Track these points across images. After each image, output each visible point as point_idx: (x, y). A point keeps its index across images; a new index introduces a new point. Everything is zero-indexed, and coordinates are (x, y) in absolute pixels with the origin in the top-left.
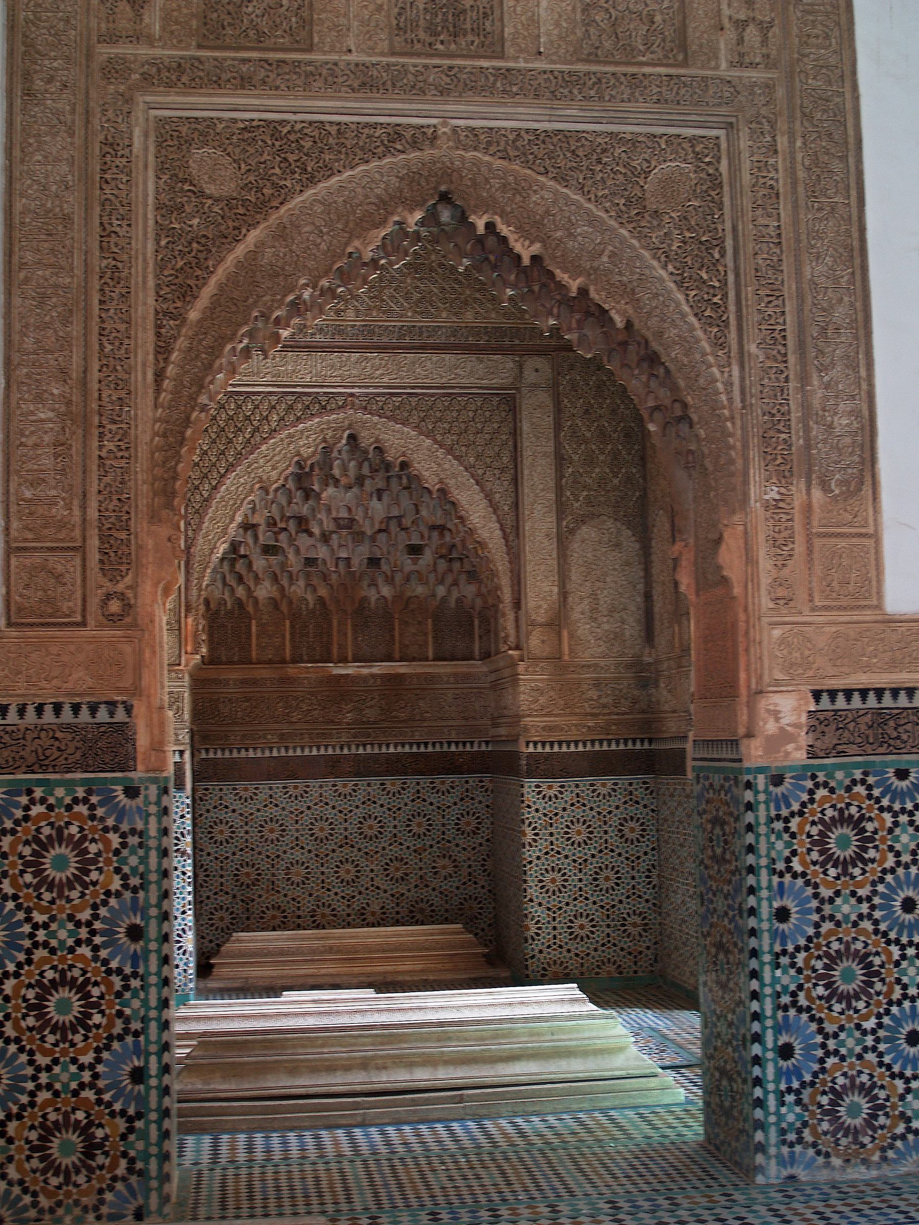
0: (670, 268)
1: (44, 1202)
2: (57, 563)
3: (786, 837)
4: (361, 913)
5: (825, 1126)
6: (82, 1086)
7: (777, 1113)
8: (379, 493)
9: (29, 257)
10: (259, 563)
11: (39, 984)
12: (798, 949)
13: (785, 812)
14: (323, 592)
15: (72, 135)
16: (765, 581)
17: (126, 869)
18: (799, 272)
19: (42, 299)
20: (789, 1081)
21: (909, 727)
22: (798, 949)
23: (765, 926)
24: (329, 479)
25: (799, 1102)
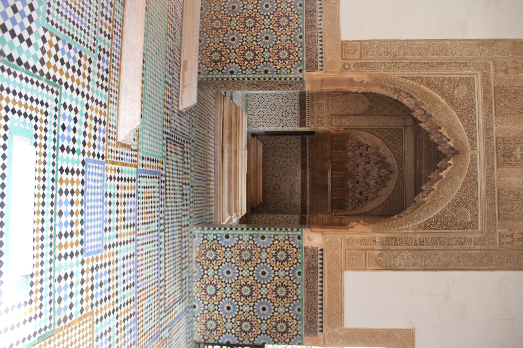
0: (440, 214)
1: (204, 52)
2: (358, 53)
3: (284, 240)
4: (266, 178)
5: (207, 247)
6: (230, 60)
7: (211, 233)
8: (376, 183)
9: (436, 45)
11: (255, 50)
12: (254, 241)
13: (290, 239)
14: (350, 169)
15: (468, 55)
16: (354, 236)
17: (282, 69)
18: (440, 250)
19: (425, 49)
20: (220, 237)
21: (312, 276)
22: (254, 241)
23: (260, 233)
24: (380, 168)
25: (214, 239)
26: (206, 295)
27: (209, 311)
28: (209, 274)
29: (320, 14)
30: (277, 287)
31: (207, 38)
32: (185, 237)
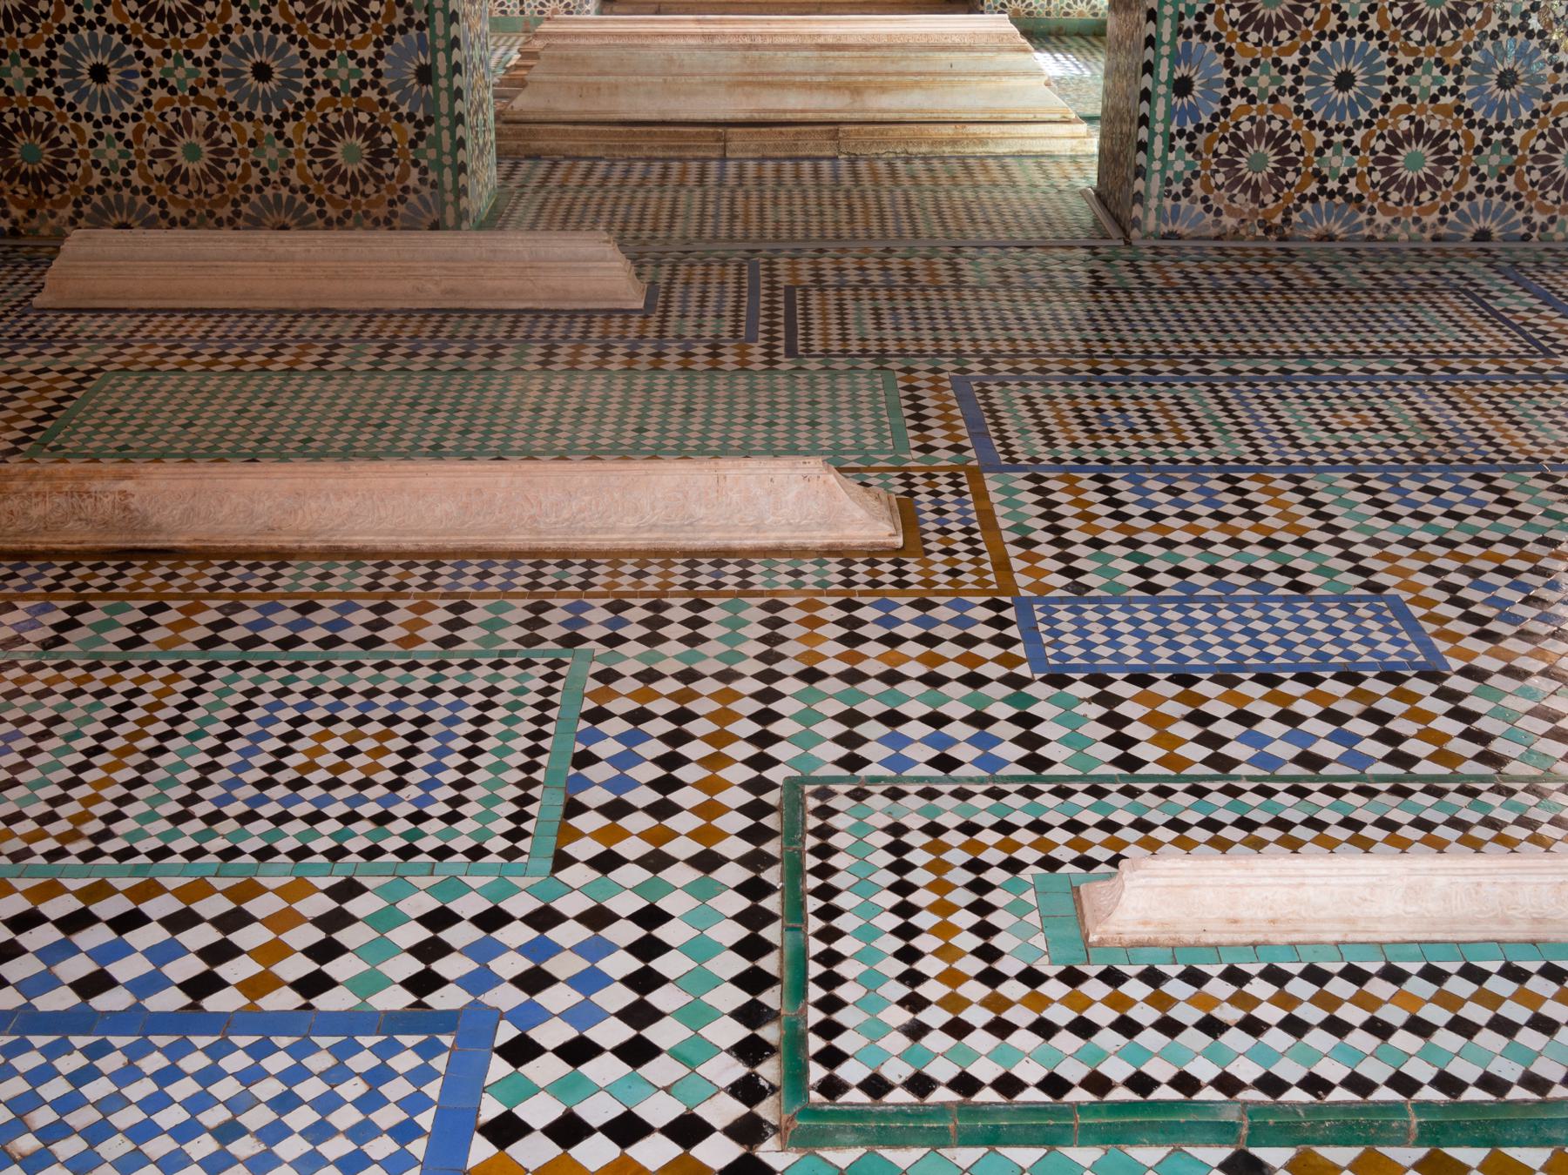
5: (1220, 178)
6: (363, 84)
20: (1182, 122)
26: (1437, 186)
27: (1511, 170)
28: (1344, 171)
31: (264, 199)
32: (1187, 276)
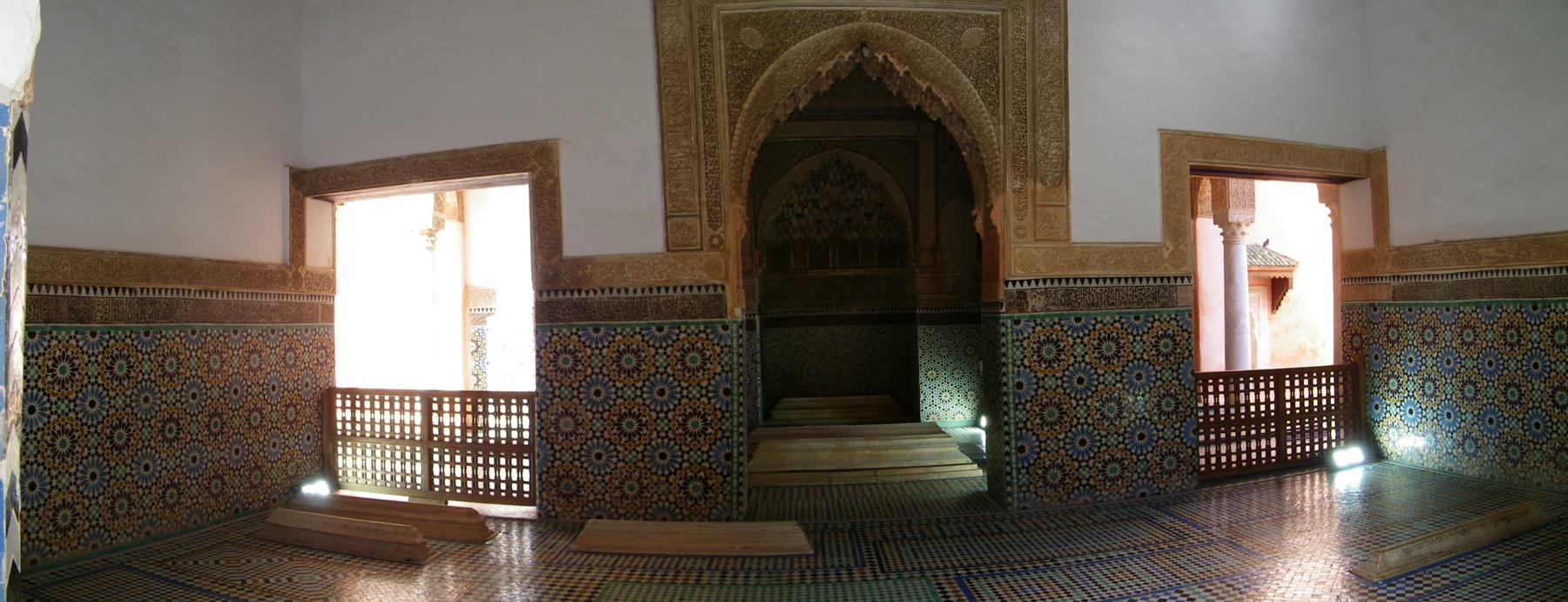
10: (795, 222)
14: (826, 235)
29: (615, 293)
30: (1102, 356)
